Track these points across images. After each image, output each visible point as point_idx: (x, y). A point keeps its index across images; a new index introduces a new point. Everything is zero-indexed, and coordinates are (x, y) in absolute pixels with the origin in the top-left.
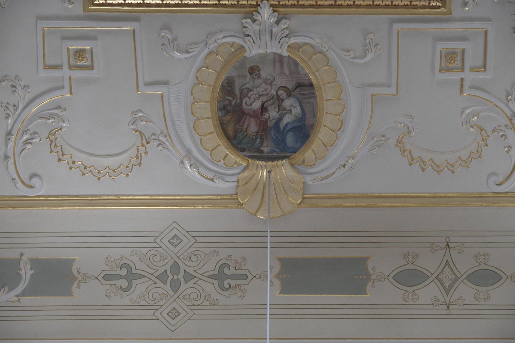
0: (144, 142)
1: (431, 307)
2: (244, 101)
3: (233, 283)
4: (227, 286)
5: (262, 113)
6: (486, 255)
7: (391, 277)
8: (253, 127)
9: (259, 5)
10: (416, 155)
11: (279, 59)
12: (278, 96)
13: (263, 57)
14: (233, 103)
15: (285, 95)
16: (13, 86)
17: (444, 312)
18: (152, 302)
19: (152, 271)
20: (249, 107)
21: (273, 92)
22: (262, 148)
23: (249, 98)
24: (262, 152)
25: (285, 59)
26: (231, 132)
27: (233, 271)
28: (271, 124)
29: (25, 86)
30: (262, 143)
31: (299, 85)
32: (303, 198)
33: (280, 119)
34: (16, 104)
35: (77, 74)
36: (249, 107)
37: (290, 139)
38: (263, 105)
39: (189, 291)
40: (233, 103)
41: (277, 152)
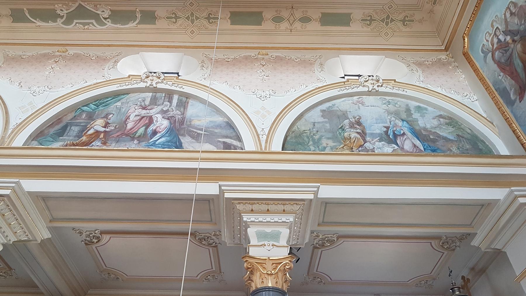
1: (285, 31)
3: (213, 21)
4: (211, 22)
6: (306, 11)
7: (271, 19)
17: (289, 33)
18: (185, 28)
19: (184, 16)
27: (213, 16)
39: (197, 24)
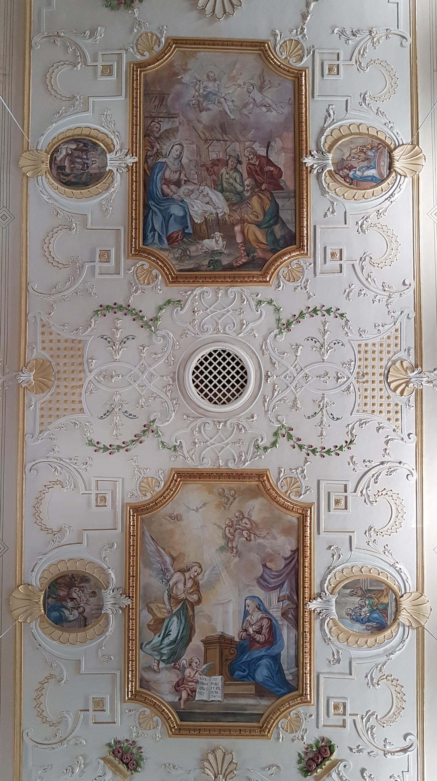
0: (55, 533)
2: (77, 588)
5: (70, 598)
8: (62, 593)
9: (129, 598)
10: (45, 686)
11: (100, 607)
12: (80, 607)
13: (101, 599)
14: (76, 582)
15: (80, 611)
16: (87, 463)
20: (73, 591)
21: (82, 605)
22: (50, 598)
23: (79, 591)
24: (48, 599)
25: (100, 611)
26: (59, 581)
28: (64, 603)
29: (86, 469)
30: (53, 598)
31: (85, 619)
32: (21, 622)
33: (67, 608)
34: (76, 464)
35: (93, 497)
36: (73, 591)
37: (55, 614)
38: (75, 599)
40: (76, 582)
41: (48, 607)
